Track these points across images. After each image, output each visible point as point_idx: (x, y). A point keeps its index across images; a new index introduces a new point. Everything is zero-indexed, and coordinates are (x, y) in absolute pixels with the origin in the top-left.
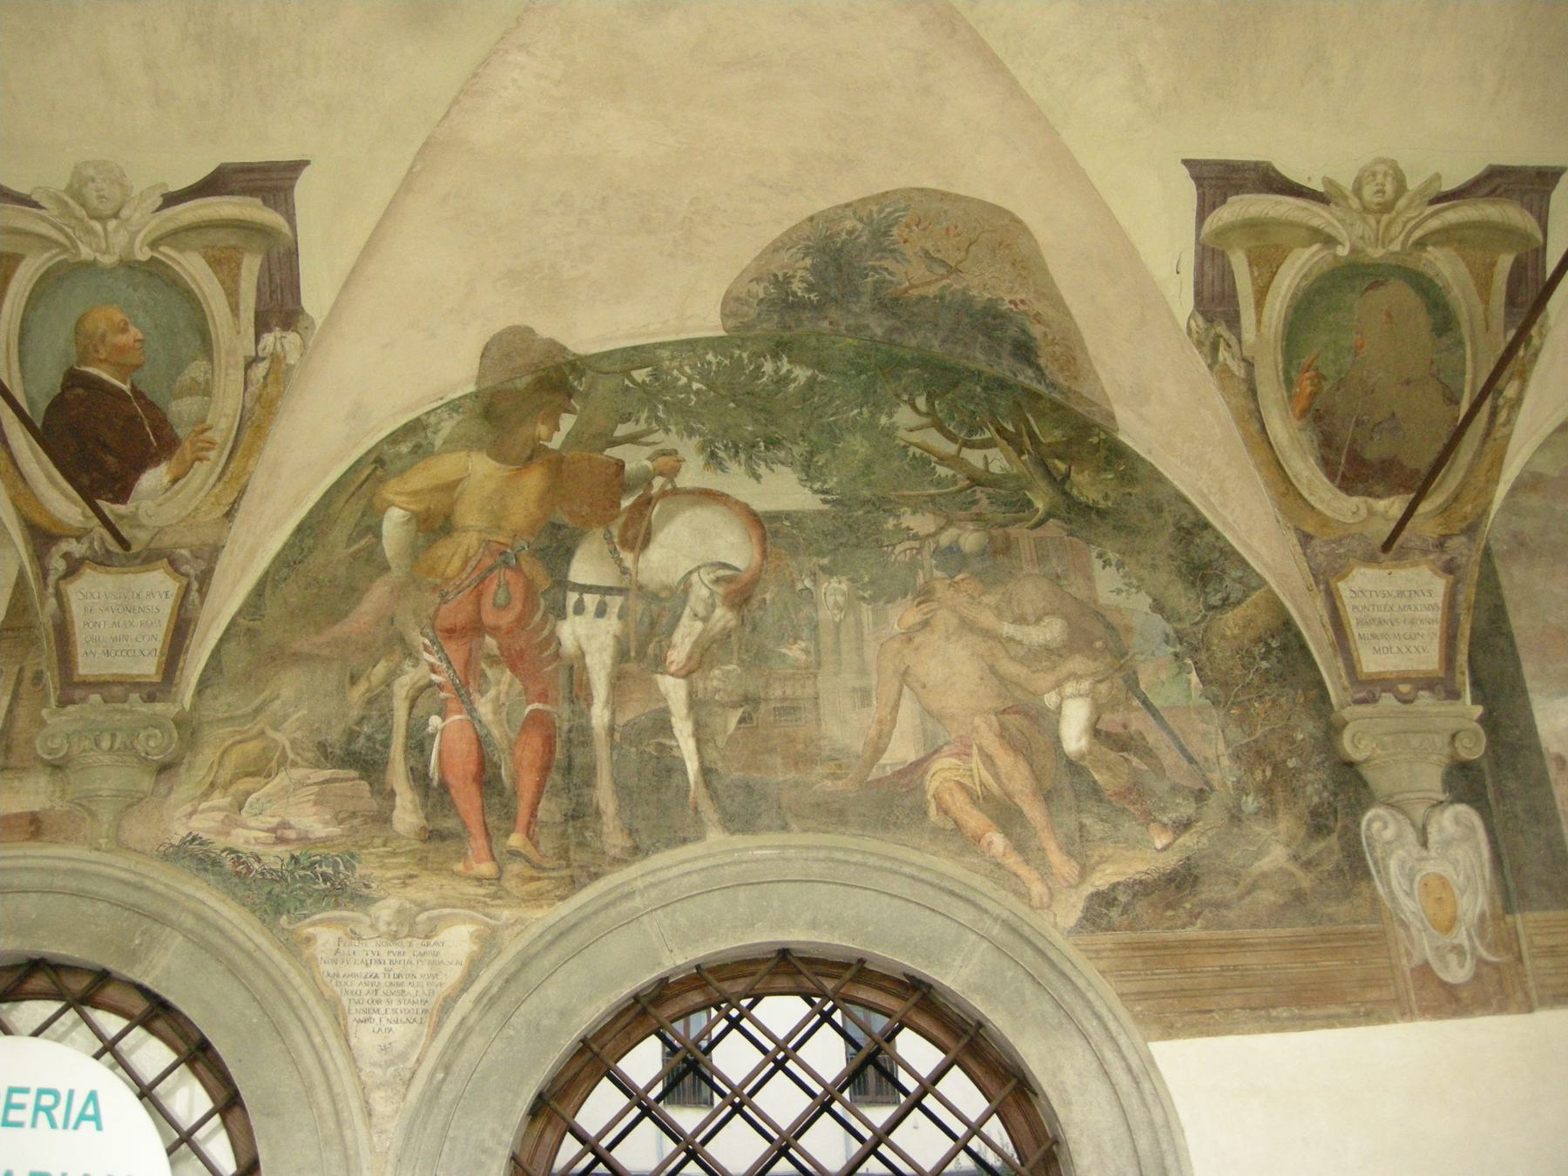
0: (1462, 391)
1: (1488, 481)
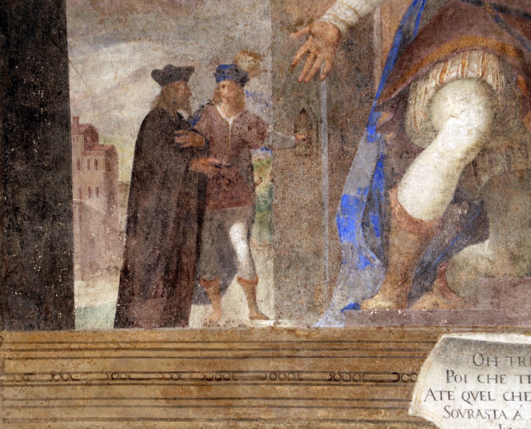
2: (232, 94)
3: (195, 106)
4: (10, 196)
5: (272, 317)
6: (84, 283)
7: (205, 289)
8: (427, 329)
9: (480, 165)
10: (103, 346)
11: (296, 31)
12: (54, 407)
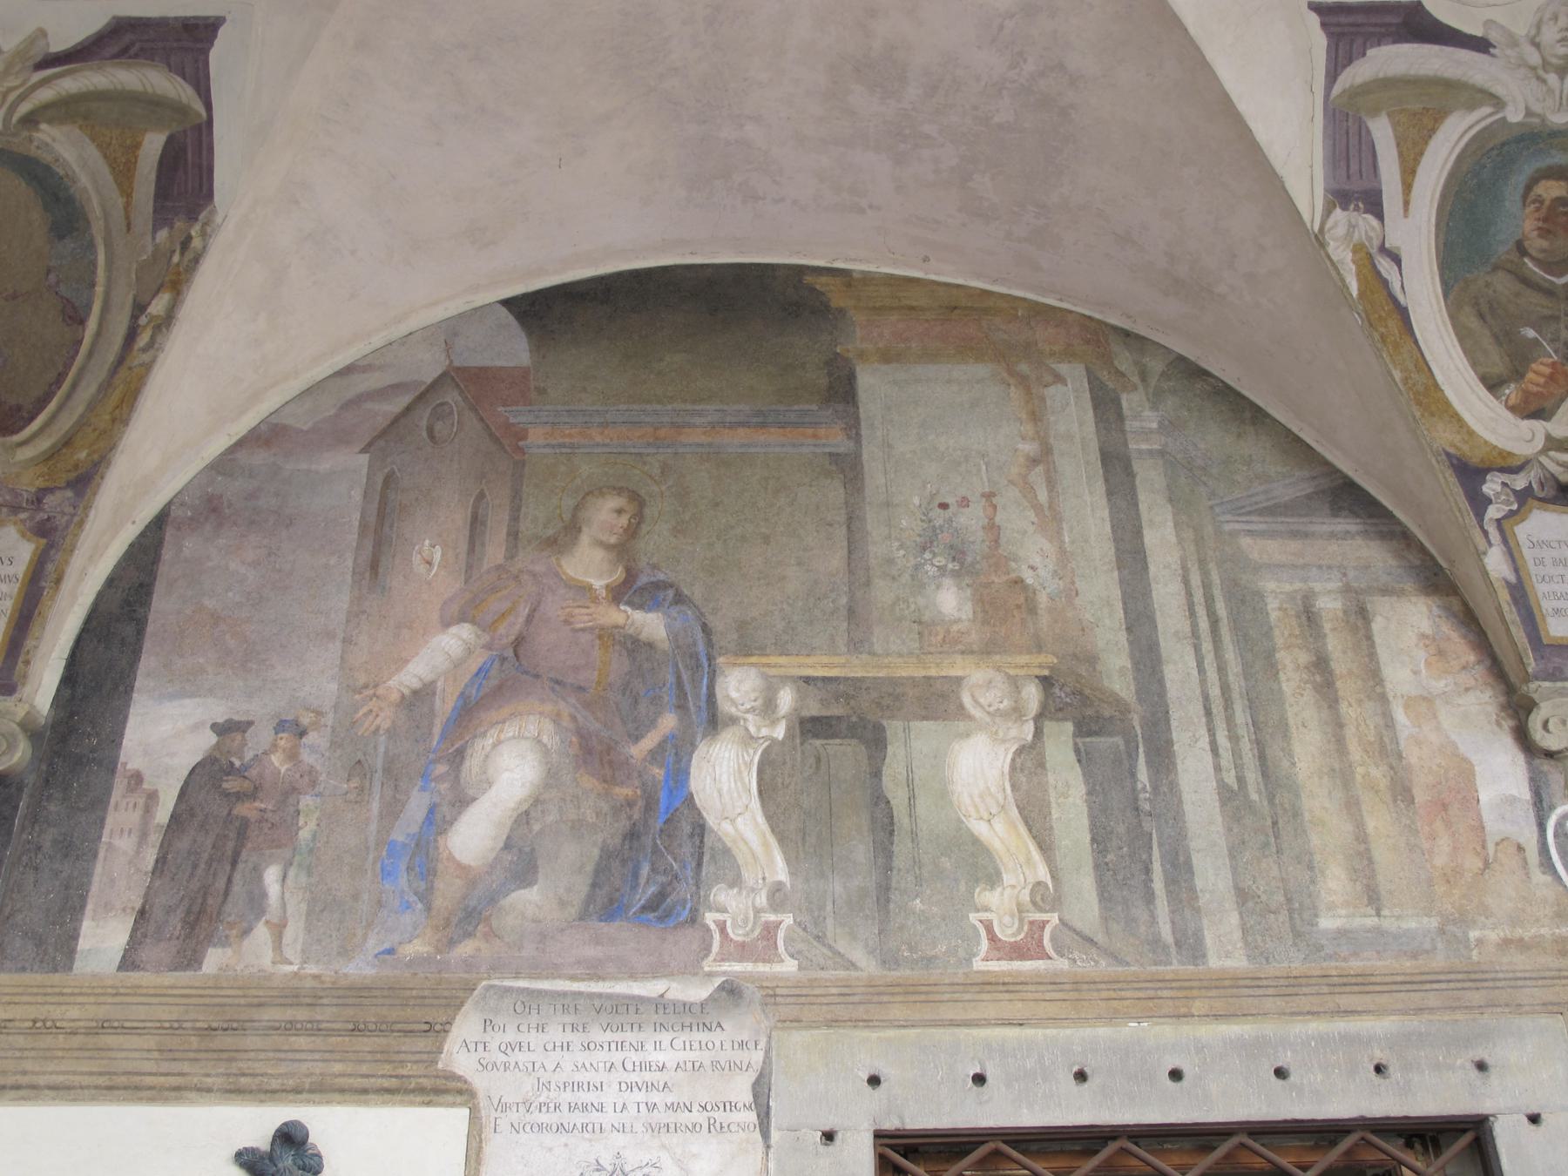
0: (89, 306)
1: (114, 420)
2: (289, 745)
3: (249, 755)
4: (35, 835)
5: (297, 961)
6: (93, 924)
7: (227, 932)
8: (466, 976)
9: (533, 814)
10: (100, 991)
11: (360, 693)
12: (27, 1058)
